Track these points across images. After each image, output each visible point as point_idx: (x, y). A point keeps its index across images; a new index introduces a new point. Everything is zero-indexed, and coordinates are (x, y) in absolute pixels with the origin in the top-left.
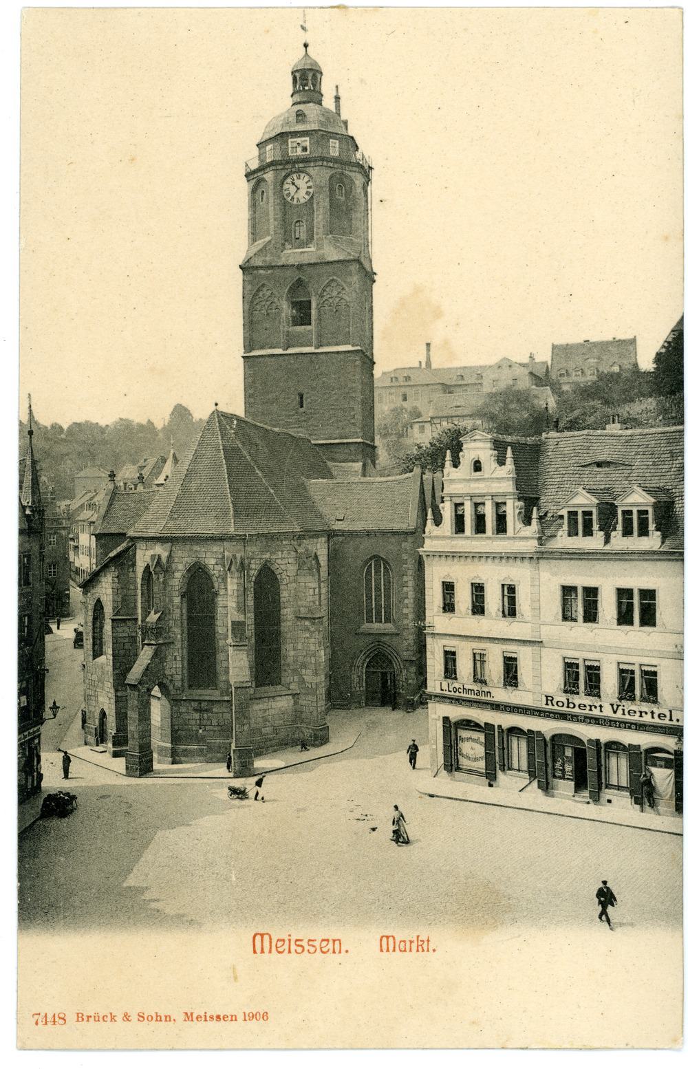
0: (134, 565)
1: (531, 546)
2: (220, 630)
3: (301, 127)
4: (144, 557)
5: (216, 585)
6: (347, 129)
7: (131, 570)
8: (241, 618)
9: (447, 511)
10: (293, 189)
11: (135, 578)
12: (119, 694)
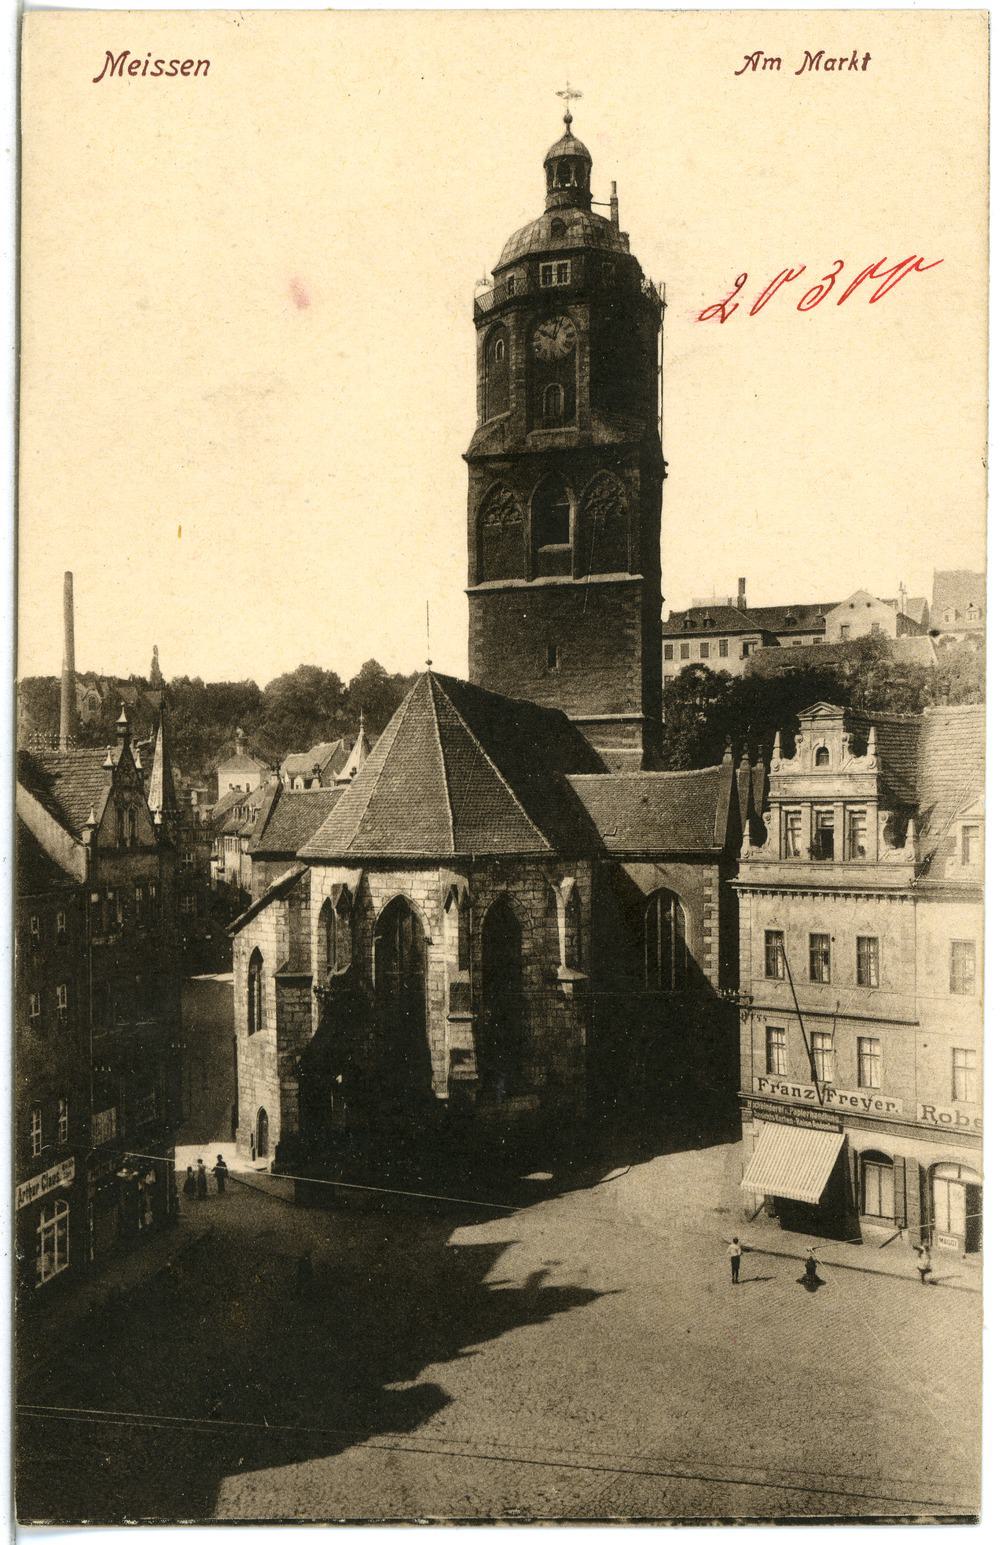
0: (307, 899)
2: (432, 996)
3: (558, 245)
5: (427, 928)
6: (627, 243)
7: (303, 906)
8: (464, 977)
9: (773, 821)
11: (309, 919)
12: (287, 1086)
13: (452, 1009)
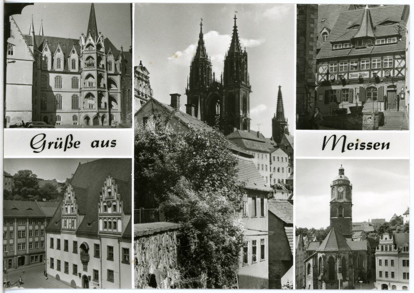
0: (317, 257)
1: (397, 253)
4: (320, 255)
8: (340, 267)
9: (380, 248)
10: (340, 189)
13: (339, 271)
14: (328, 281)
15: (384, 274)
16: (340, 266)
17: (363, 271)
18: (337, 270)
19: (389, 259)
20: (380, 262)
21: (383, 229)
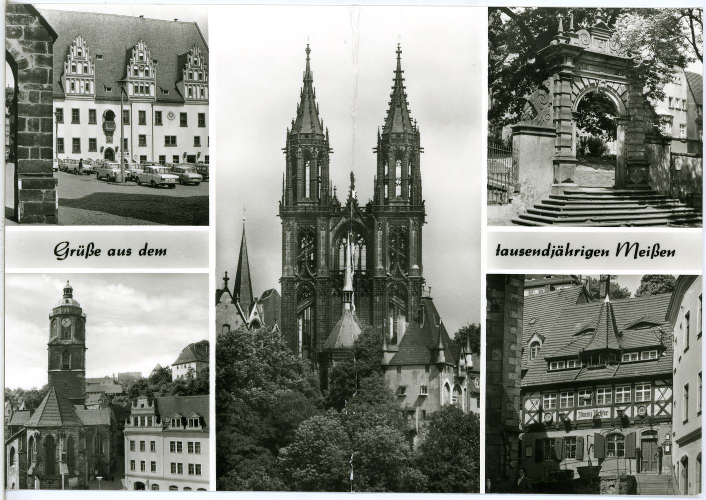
0: (26, 436)
1: (160, 430)
4: (30, 433)
8: (64, 453)
14: (44, 476)
15: (138, 465)
16: (64, 451)
17: (104, 459)
18: (59, 459)
19: (148, 439)
20: (131, 445)
21: (137, 390)
